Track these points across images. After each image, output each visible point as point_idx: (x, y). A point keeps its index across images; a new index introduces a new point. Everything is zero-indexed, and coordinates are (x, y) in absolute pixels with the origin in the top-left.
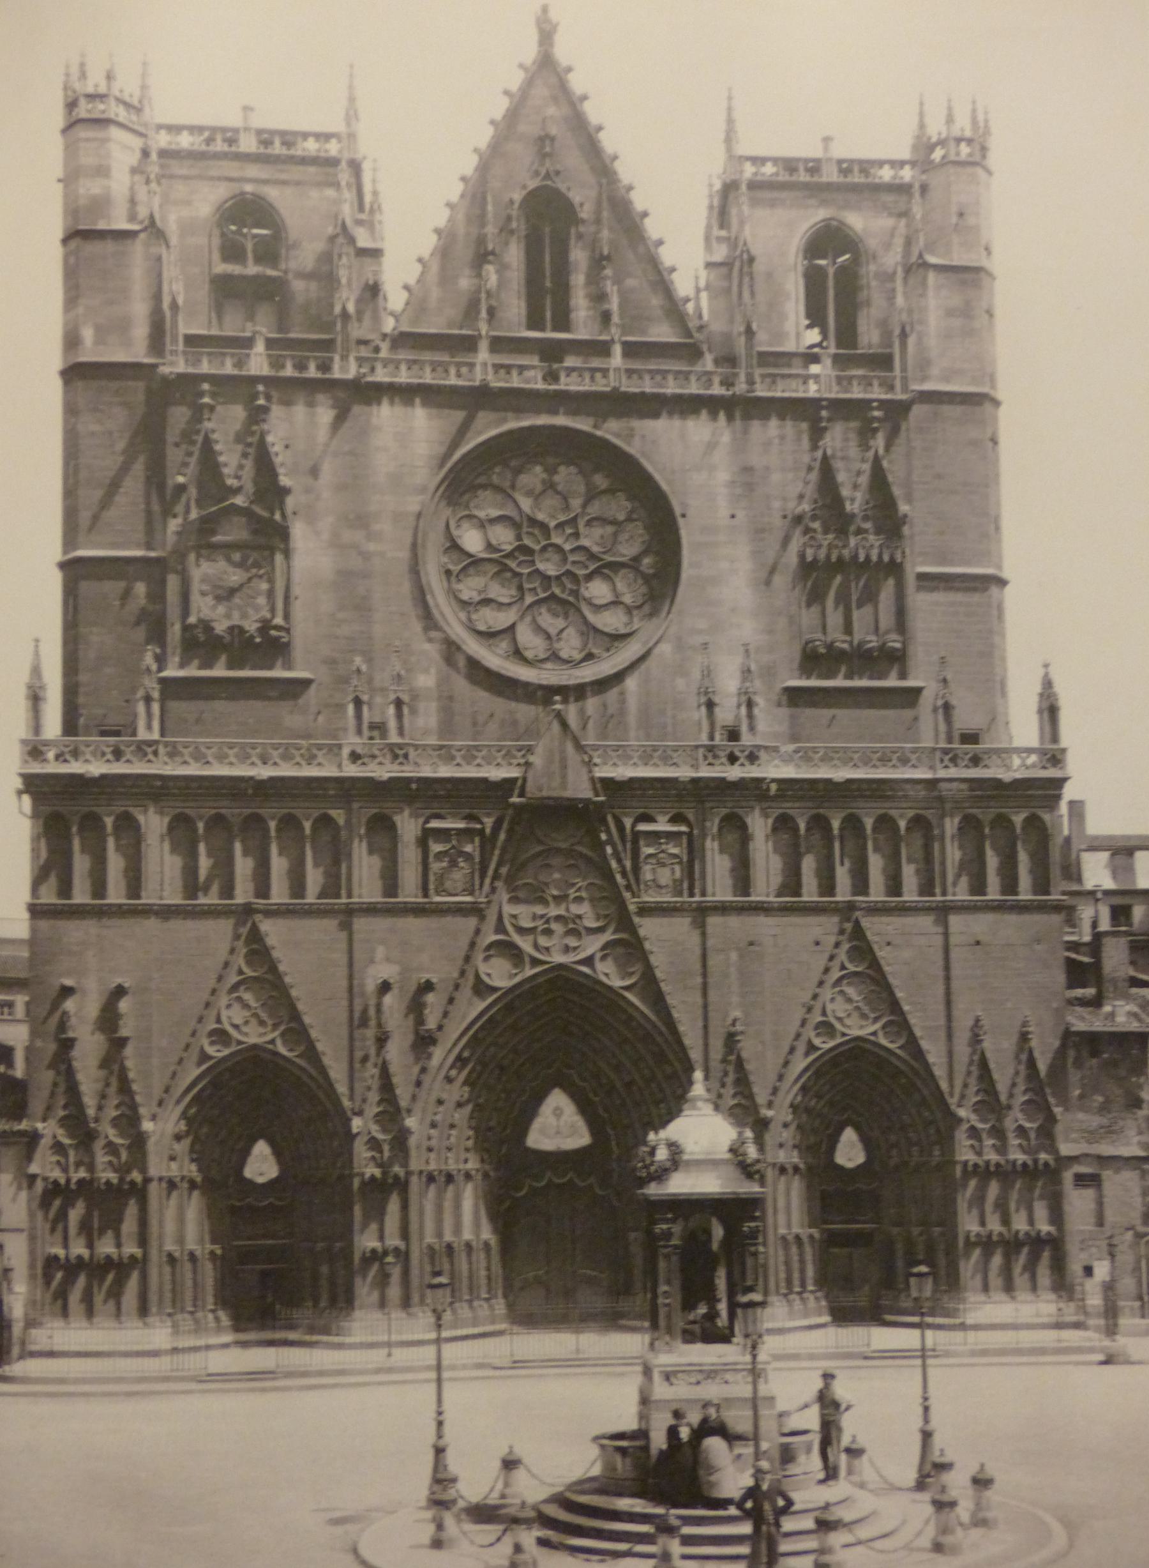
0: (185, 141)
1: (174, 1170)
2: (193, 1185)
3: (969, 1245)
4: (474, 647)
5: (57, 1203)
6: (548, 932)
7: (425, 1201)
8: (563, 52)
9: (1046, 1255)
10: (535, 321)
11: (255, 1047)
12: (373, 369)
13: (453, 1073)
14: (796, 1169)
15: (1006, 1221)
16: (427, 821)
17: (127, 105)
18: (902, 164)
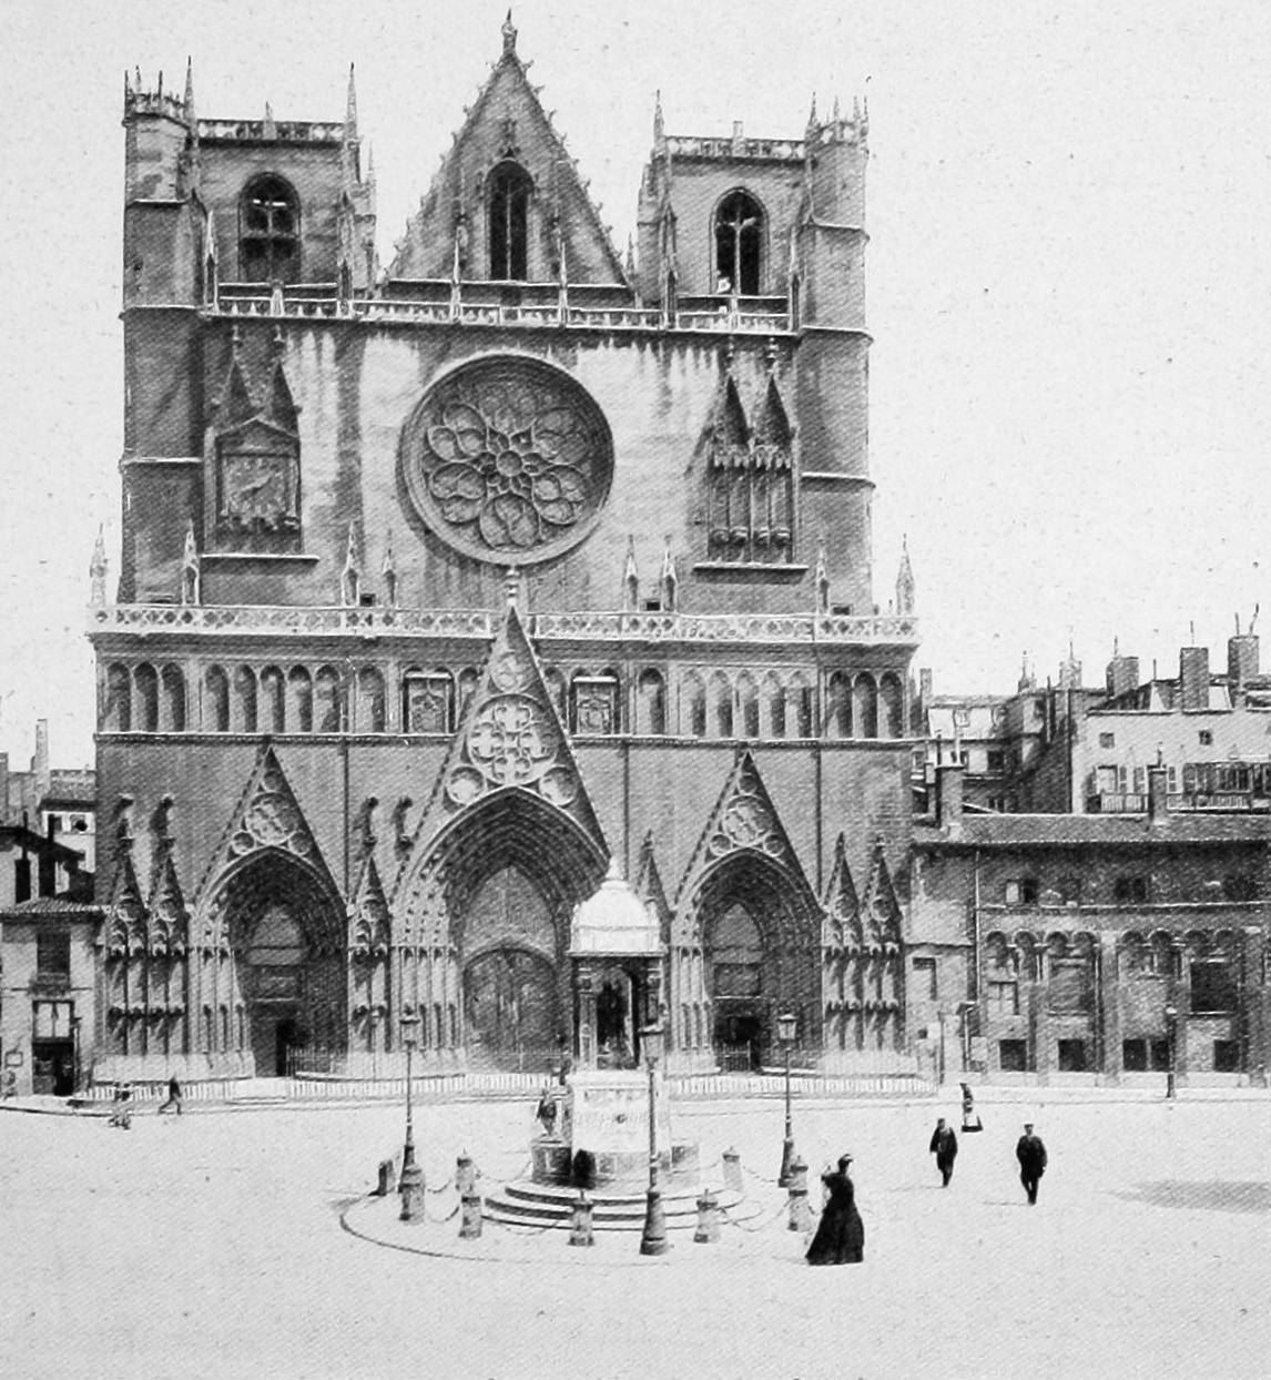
0: (220, 132)
1: (209, 942)
2: (224, 954)
3: (830, 1012)
4: (445, 534)
5: (119, 966)
6: (503, 761)
7: (403, 970)
8: (522, 54)
9: (891, 1020)
10: (497, 271)
11: (272, 848)
12: (367, 312)
13: (426, 871)
14: (696, 952)
15: (859, 993)
16: (407, 672)
17: (176, 104)
18: (797, 143)
